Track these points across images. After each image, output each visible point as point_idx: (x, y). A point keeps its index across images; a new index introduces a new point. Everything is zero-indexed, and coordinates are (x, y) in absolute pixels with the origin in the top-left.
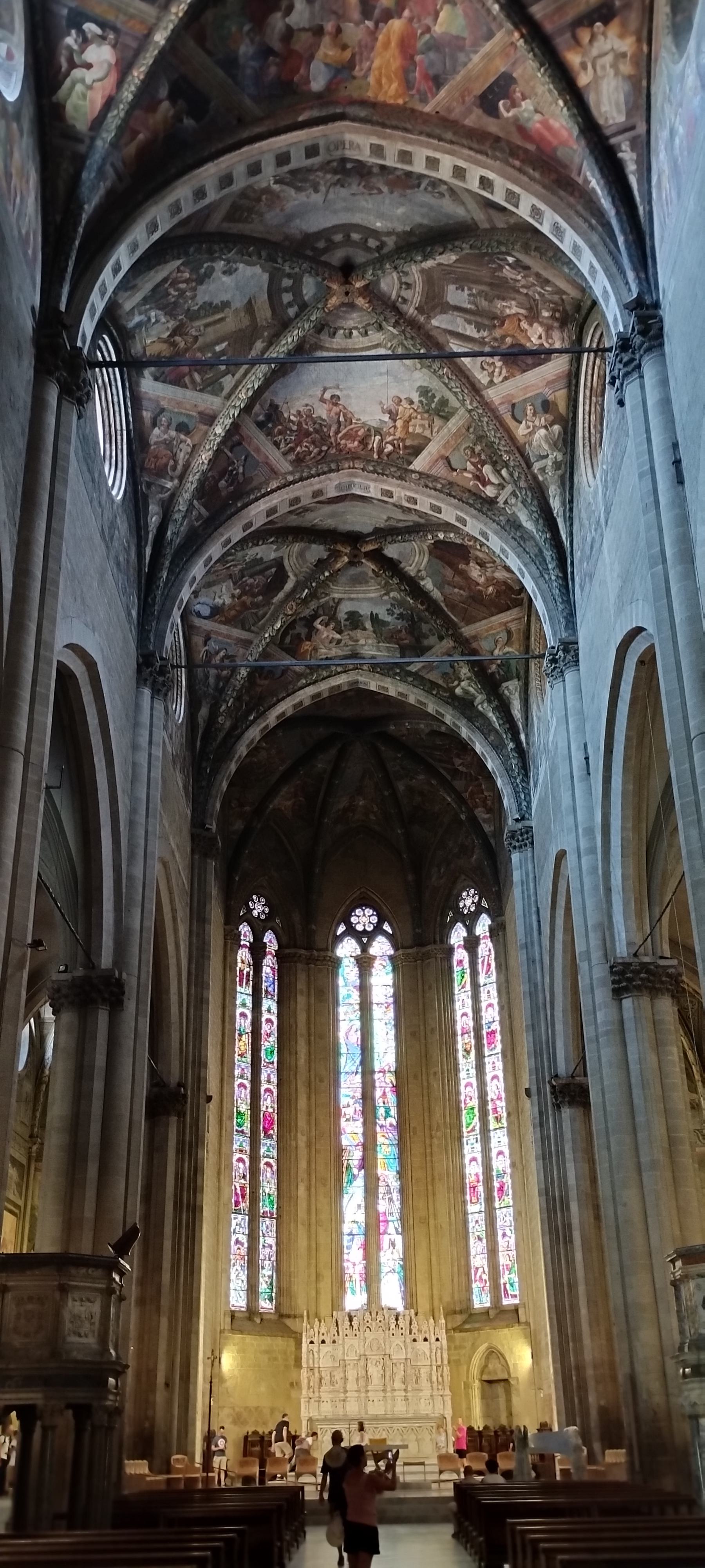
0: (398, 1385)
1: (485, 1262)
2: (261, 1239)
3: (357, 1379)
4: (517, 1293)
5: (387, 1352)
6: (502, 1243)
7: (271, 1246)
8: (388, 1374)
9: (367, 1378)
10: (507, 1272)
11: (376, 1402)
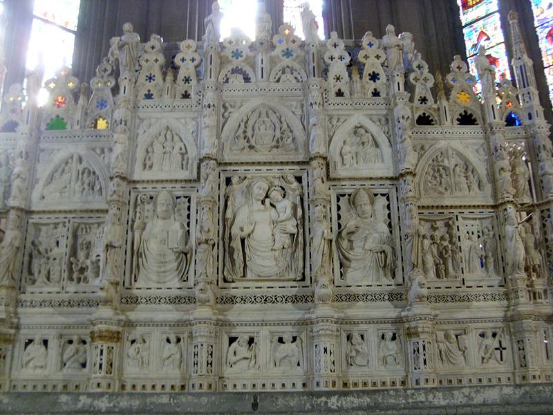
0: (362, 276)
3: (184, 256)
5: (317, 148)
8: (321, 231)
9: (230, 248)
11: (264, 347)
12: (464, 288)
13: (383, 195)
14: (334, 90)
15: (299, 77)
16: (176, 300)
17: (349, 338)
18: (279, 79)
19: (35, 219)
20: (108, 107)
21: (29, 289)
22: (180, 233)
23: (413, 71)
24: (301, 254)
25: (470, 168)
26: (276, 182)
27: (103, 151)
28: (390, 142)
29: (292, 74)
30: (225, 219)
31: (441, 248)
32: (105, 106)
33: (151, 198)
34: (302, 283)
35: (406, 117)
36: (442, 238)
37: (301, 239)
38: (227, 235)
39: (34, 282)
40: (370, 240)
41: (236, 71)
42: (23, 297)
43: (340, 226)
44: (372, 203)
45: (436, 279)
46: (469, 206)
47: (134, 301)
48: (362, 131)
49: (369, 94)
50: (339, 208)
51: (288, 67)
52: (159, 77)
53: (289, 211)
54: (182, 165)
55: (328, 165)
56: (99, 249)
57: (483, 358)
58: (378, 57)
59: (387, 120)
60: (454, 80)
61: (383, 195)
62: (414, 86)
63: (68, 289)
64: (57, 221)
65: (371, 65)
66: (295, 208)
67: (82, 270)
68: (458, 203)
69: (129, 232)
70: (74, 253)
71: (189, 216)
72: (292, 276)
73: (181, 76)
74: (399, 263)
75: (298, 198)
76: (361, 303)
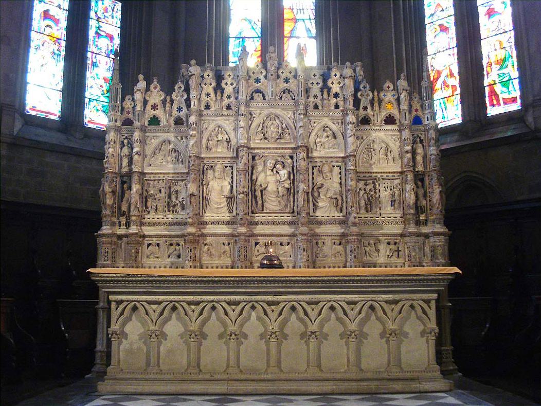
1: (454, 60)
2: (93, 23)
3: (230, 199)
4: (517, 93)
6: (486, 26)
7: (111, 38)
10: (495, 67)
12: (380, 218)
13: (338, 166)
14: (312, 105)
15: (293, 96)
16: (228, 223)
17: (317, 243)
18: (282, 97)
19: (147, 177)
20: (183, 111)
21: (147, 216)
22: (229, 187)
23: (360, 90)
24: (292, 199)
25: (389, 150)
26: (279, 159)
27: (182, 139)
28: (343, 136)
29: (289, 93)
30: (252, 180)
31: (369, 196)
32: (182, 111)
33: (212, 167)
34: (293, 215)
35: (352, 122)
36: (370, 190)
37: (292, 191)
38: (253, 189)
39: (149, 212)
40: (329, 192)
41: (258, 91)
42: (143, 221)
43: (313, 183)
44: (331, 171)
45: (365, 212)
46: (387, 173)
47: (205, 223)
48: (328, 129)
49: (333, 108)
50: (313, 173)
51: (287, 89)
52: (212, 95)
53: (286, 176)
54: (228, 148)
55: (308, 150)
56: (182, 195)
57: (388, 256)
58: (339, 83)
59: (342, 122)
60: (385, 95)
61: (338, 166)
62: (360, 100)
63: (168, 216)
64: (160, 178)
65: (336, 88)
66: (289, 173)
67: (174, 206)
68: (380, 171)
69: (201, 187)
70: (170, 197)
71: (232, 178)
72: (288, 210)
73: (225, 95)
74: (344, 204)
75: (291, 169)
76: (324, 226)
